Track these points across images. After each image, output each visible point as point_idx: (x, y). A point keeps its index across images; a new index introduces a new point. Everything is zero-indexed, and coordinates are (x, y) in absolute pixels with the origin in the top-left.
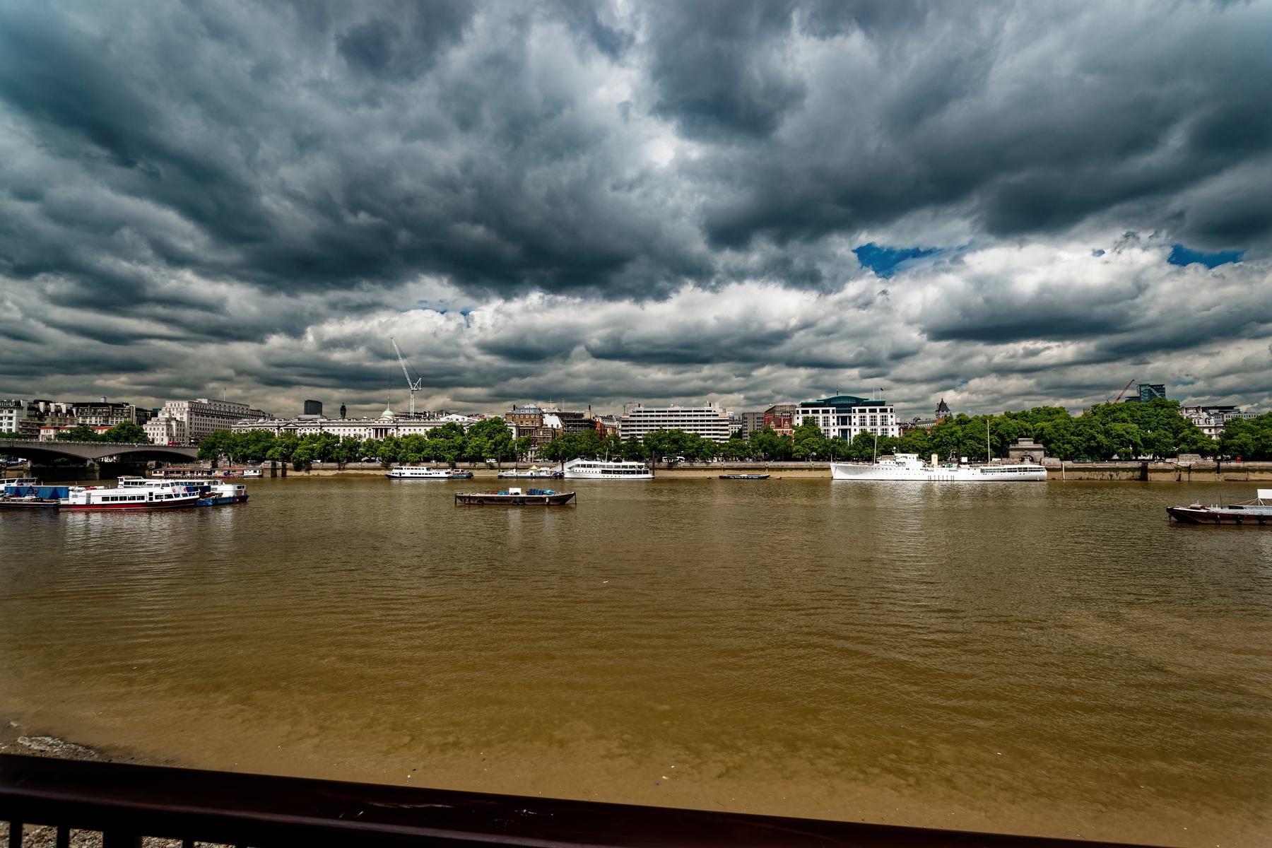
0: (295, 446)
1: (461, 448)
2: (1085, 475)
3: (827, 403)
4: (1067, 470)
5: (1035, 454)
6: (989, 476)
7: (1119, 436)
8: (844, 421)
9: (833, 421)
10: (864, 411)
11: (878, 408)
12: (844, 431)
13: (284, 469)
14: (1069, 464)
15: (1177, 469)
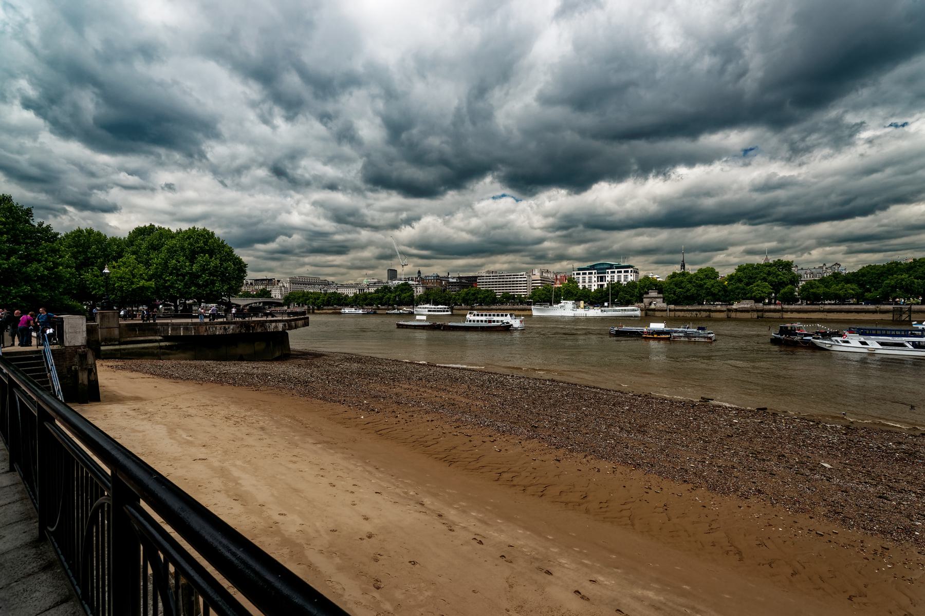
0: (318, 298)
1: (382, 298)
2: (681, 314)
3: (592, 267)
4: (670, 310)
5: (658, 300)
6: (605, 314)
7: (707, 288)
8: (602, 279)
9: (594, 279)
10: (614, 272)
11: (623, 270)
12: (602, 286)
13: (313, 309)
14: (672, 307)
15: (729, 310)
